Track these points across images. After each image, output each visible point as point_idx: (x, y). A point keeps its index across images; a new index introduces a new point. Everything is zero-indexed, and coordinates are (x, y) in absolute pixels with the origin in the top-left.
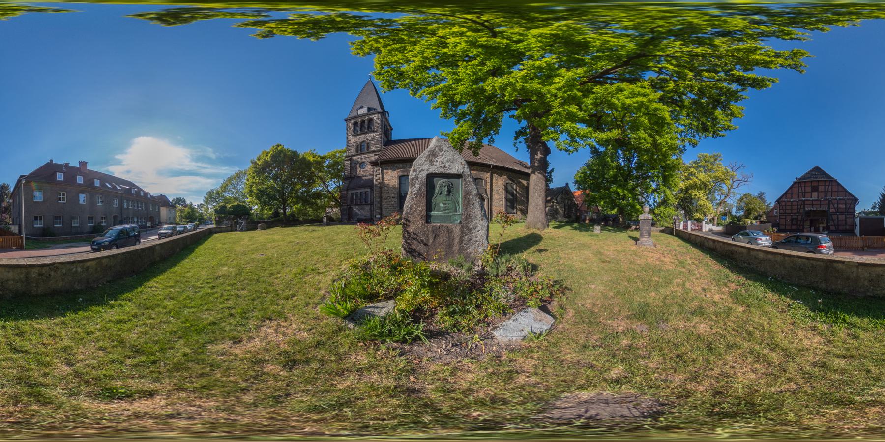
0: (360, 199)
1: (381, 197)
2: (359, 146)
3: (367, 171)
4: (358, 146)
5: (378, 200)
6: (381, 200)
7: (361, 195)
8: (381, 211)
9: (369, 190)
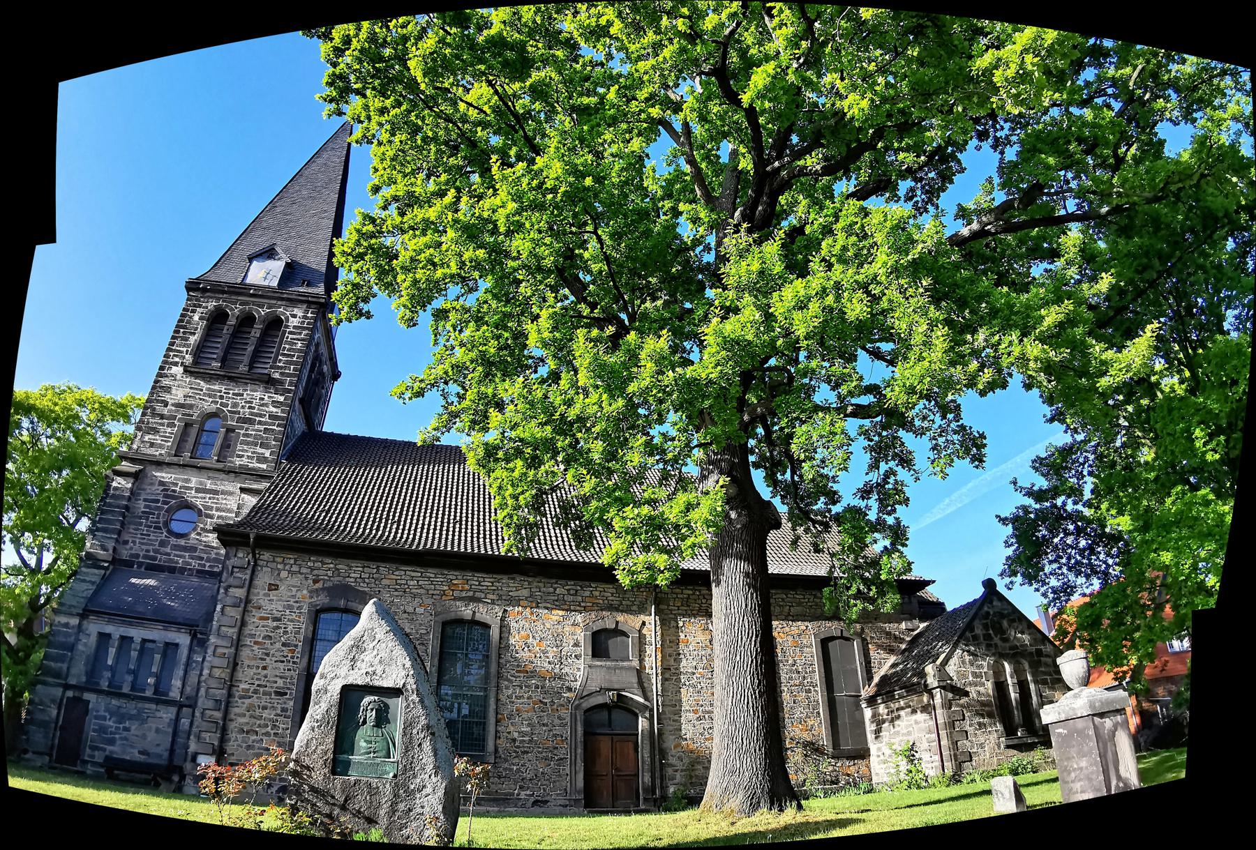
0: (134, 673)
1: (231, 684)
2: (193, 432)
3: (193, 549)
4: (188, 425)
5: (221, 693)
6: (230, 695)
7: (142, 651)
8: (223, 739)
9: (183, 639)
